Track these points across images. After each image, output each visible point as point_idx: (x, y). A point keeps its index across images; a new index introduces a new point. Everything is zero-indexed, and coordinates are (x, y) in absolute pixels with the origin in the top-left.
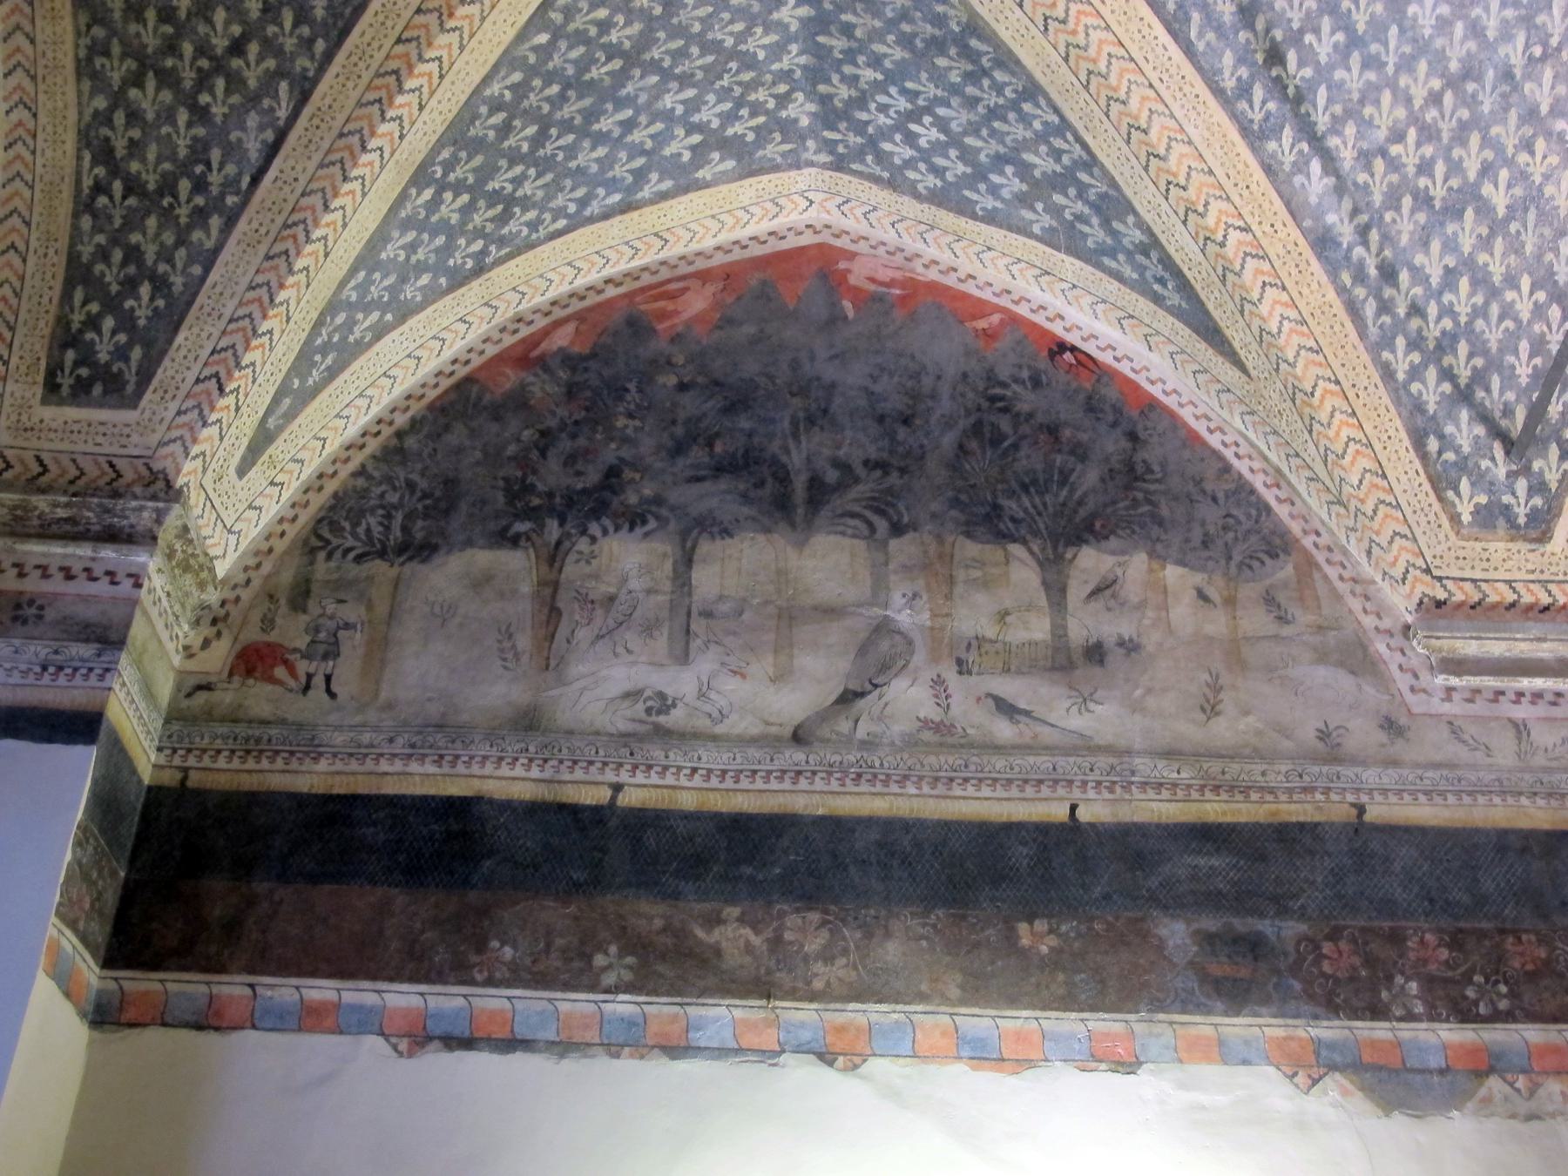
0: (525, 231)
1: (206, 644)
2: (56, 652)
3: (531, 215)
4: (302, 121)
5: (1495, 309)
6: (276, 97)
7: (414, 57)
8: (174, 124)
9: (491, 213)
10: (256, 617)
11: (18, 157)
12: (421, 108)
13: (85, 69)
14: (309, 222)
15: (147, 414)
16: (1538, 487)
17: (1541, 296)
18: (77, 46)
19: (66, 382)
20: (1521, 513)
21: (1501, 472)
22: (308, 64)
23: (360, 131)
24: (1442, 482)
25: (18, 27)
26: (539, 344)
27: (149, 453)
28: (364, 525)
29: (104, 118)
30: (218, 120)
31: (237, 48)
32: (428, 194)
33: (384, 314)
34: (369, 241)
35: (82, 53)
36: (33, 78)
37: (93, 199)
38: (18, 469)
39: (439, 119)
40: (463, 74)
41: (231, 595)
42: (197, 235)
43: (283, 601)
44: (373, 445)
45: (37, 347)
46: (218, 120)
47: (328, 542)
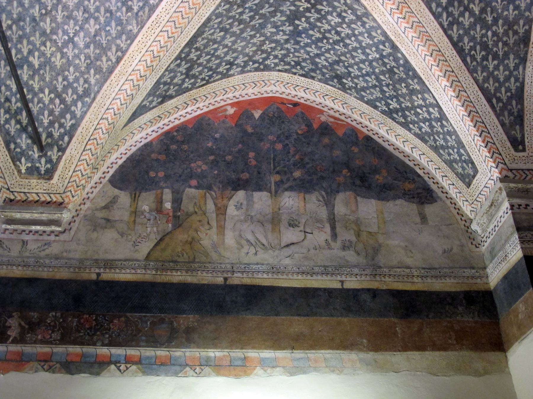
5: (36, 100)
16: (49, 161)
17: (52, 96)
20: (43, 170)
21: (36, 156)
24: (15, 159)
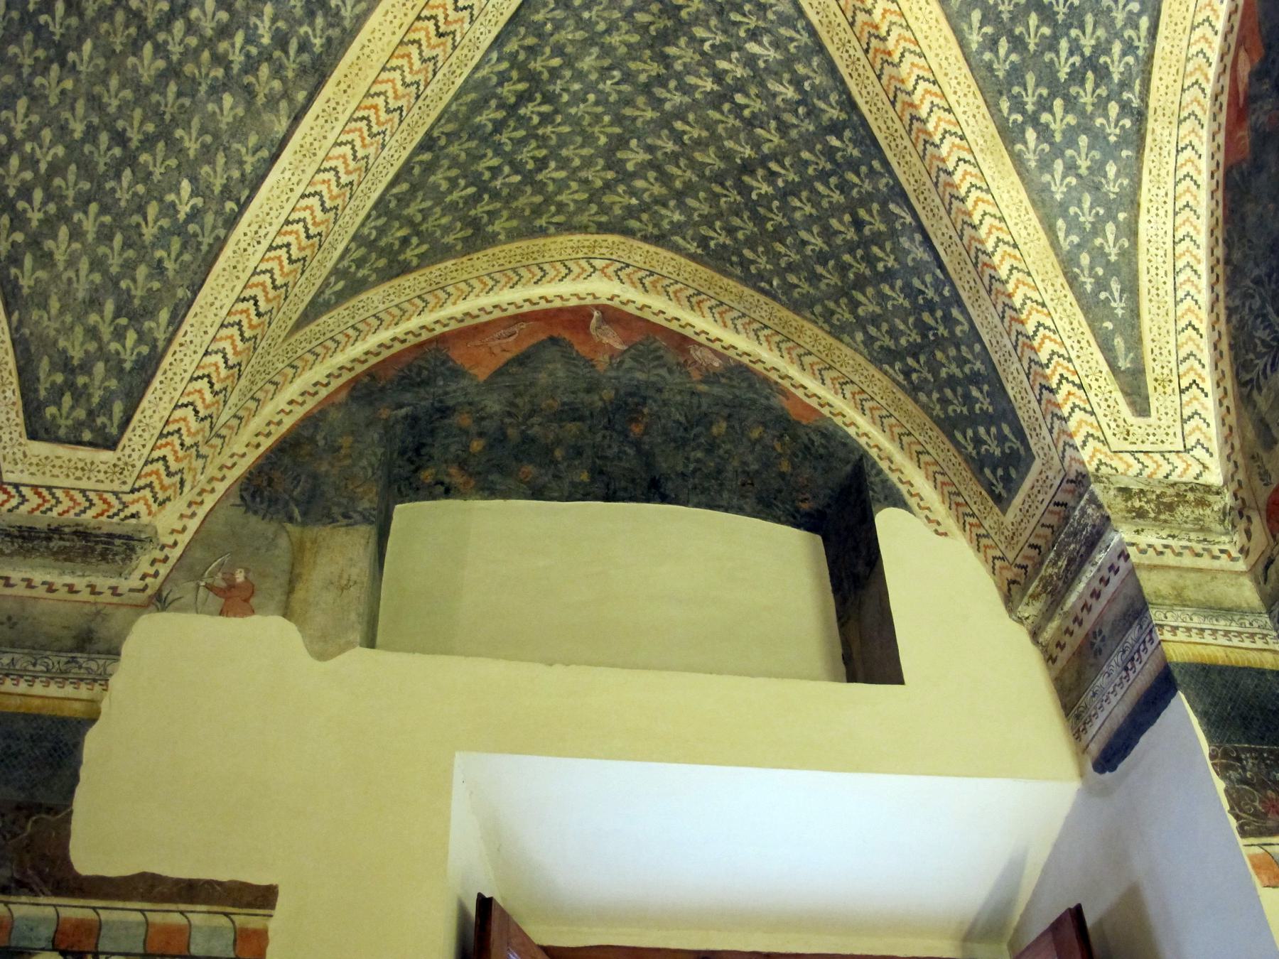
0: (1130, 59)
1: (1248, 533)
2: (1124, 651)
3: (1117, 48)
4: (918, 208)
6: (898, 217)
7: (907, 98)
8: (889, 298)
9: (1089, 85)
10: (1257, 483)
11: (871, 409)
12: (950, 110)
13: (837, 332)
14: (979, 246)
15: (1041, 453)
18: (821, 328)
19: (999, 488)
22: (884, 181)
23: (939, 169)
25: (800, 356)
26: (1237, 92)
27: (1062, 473)
28: (1258, 341)
29: (869, 341)
30: (897, 266)
31: (858, 224)
32: (1031, 135)
33: (1115, 219)
34: (1033, 203)
35: (826, 327)
36: (830, 368)
37: (911, 382)
38: (1030, 563)
39: (970, 98)
40: (944, 64)
41: (1234, 486)
42: (958, 330)
43: (1261, 452)
44: (1221, 289)
45: (974, 488)
46: (897, 266)
47: (1251, 380)
